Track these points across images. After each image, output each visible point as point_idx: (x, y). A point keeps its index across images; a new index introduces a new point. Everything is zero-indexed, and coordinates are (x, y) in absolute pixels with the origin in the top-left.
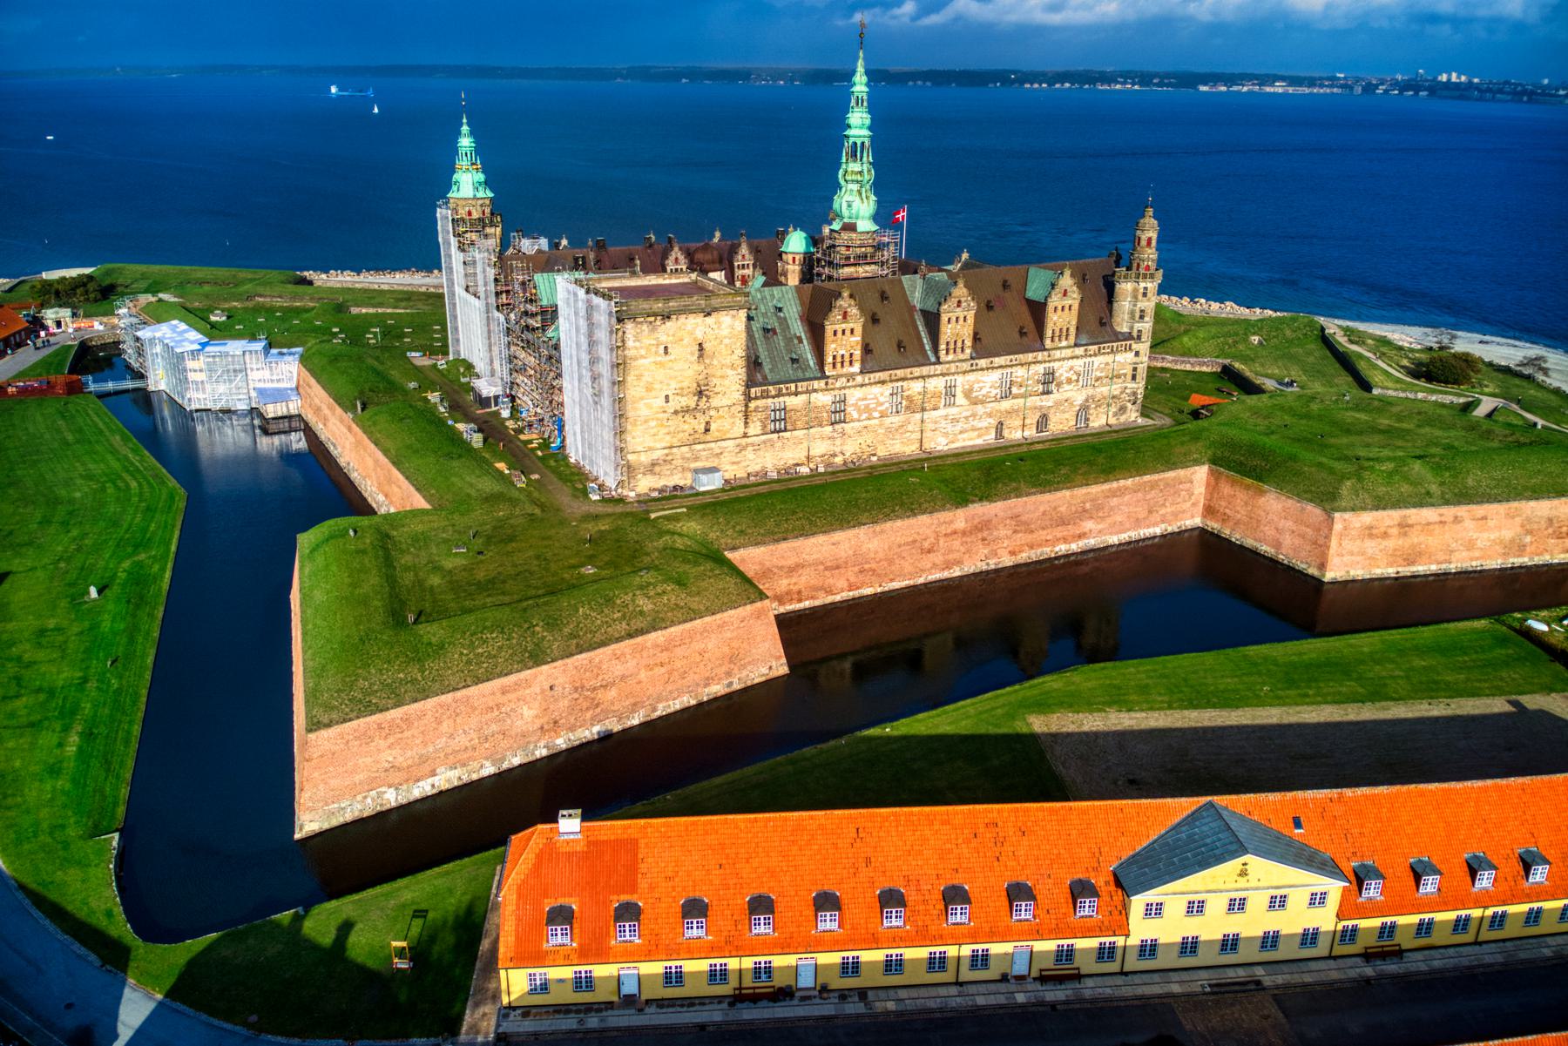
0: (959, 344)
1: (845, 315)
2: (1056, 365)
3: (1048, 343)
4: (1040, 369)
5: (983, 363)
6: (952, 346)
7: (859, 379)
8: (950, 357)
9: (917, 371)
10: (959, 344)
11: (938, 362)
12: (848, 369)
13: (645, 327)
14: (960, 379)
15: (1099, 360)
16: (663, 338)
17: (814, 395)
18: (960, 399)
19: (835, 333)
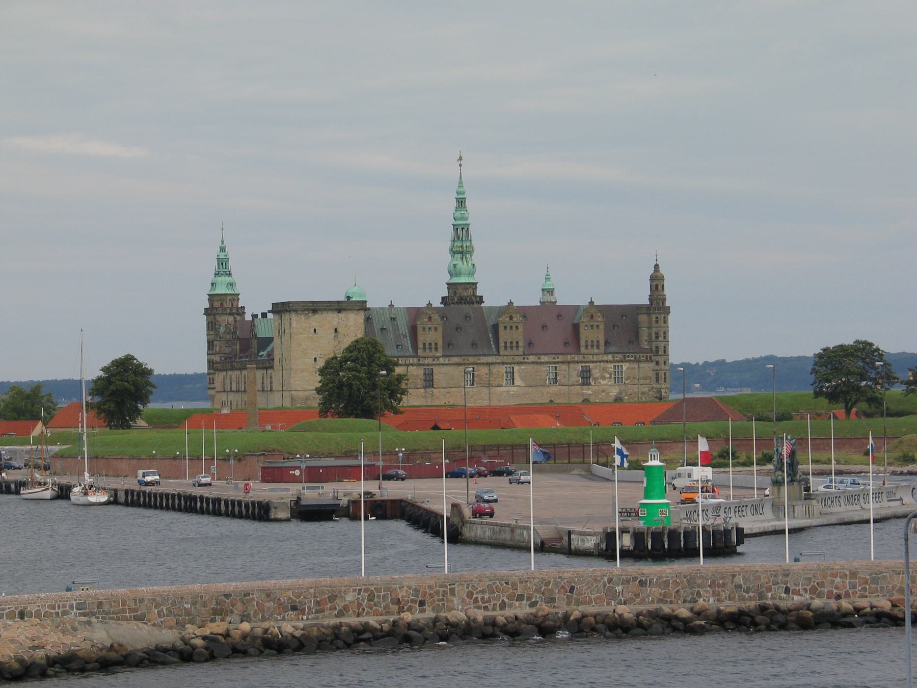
0: (514, 344)
1: (430, 319)
2: (591, 365)
3: (583, 349)
4: (579, 367)
5: (532, 358)
6: (508, 345)
7: (442, 360)
8: (506, 353)
9: (484, 360)
10: (514, 344)
11: (499, 355)
12: (434, 353)
13: (302, 317)
14: (516, 368)
15: (625, 366)
16: (314, 324)
17: (411, 368)
18: (518, 381)
19: (424, 328)
